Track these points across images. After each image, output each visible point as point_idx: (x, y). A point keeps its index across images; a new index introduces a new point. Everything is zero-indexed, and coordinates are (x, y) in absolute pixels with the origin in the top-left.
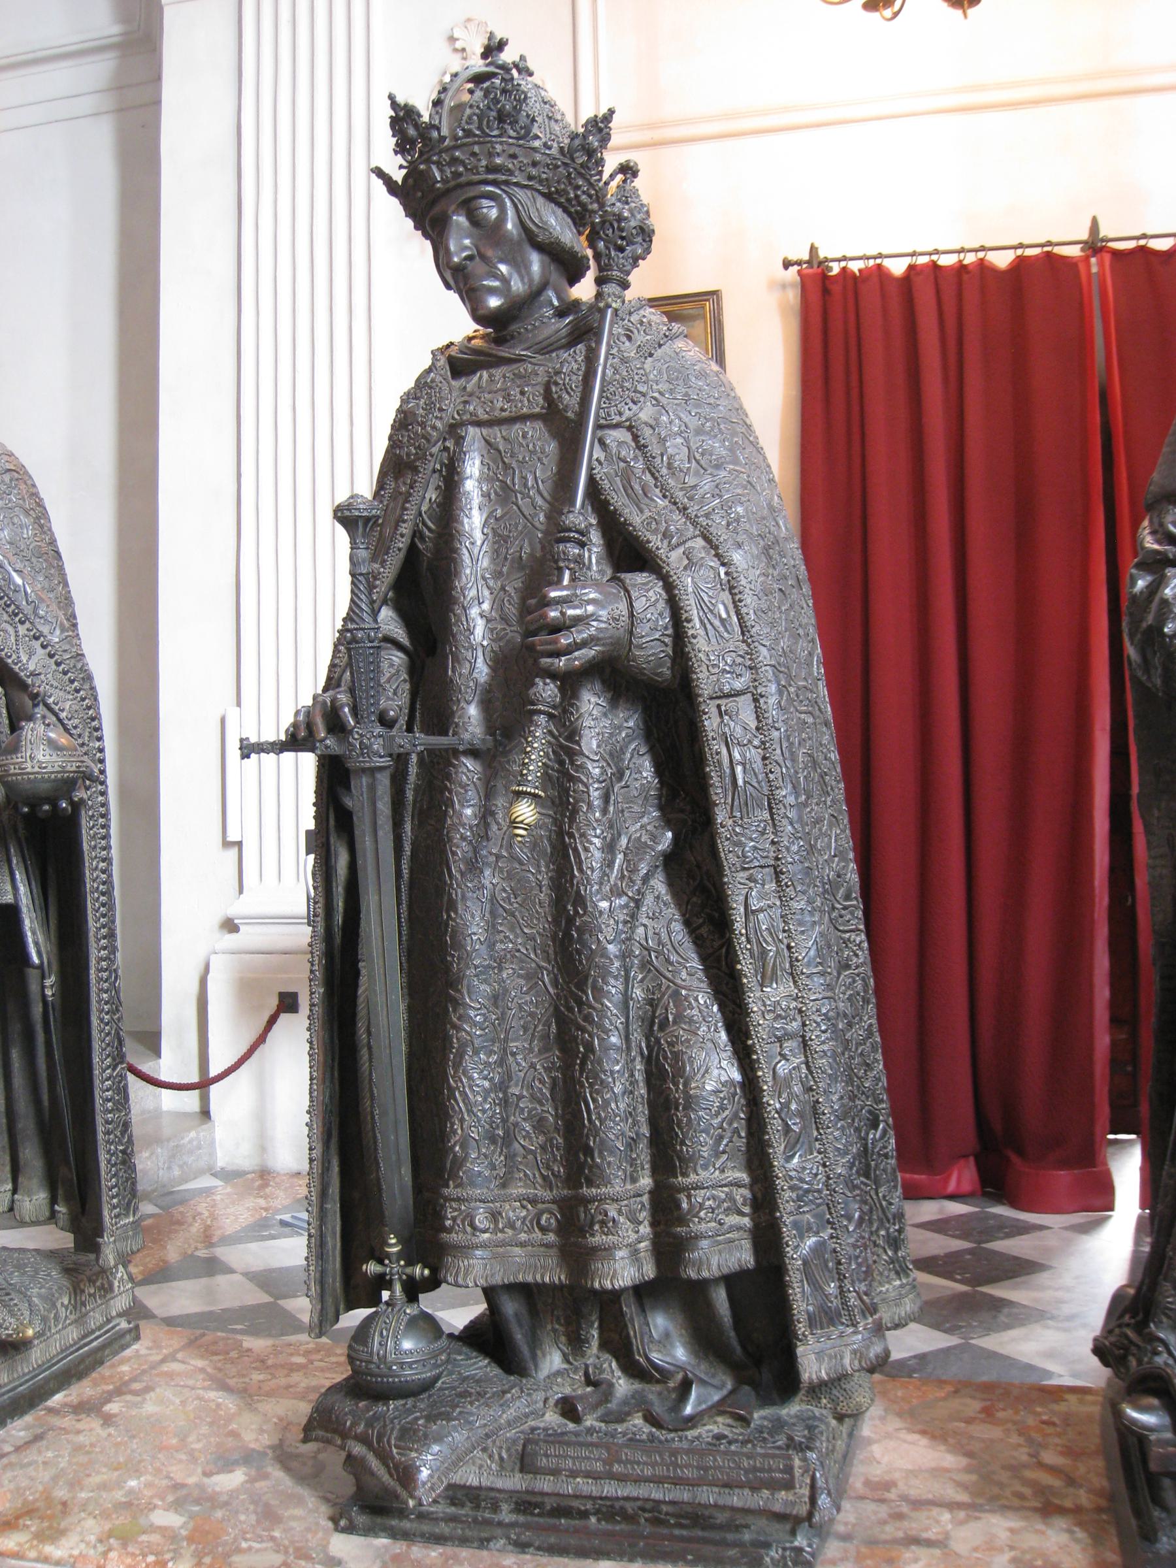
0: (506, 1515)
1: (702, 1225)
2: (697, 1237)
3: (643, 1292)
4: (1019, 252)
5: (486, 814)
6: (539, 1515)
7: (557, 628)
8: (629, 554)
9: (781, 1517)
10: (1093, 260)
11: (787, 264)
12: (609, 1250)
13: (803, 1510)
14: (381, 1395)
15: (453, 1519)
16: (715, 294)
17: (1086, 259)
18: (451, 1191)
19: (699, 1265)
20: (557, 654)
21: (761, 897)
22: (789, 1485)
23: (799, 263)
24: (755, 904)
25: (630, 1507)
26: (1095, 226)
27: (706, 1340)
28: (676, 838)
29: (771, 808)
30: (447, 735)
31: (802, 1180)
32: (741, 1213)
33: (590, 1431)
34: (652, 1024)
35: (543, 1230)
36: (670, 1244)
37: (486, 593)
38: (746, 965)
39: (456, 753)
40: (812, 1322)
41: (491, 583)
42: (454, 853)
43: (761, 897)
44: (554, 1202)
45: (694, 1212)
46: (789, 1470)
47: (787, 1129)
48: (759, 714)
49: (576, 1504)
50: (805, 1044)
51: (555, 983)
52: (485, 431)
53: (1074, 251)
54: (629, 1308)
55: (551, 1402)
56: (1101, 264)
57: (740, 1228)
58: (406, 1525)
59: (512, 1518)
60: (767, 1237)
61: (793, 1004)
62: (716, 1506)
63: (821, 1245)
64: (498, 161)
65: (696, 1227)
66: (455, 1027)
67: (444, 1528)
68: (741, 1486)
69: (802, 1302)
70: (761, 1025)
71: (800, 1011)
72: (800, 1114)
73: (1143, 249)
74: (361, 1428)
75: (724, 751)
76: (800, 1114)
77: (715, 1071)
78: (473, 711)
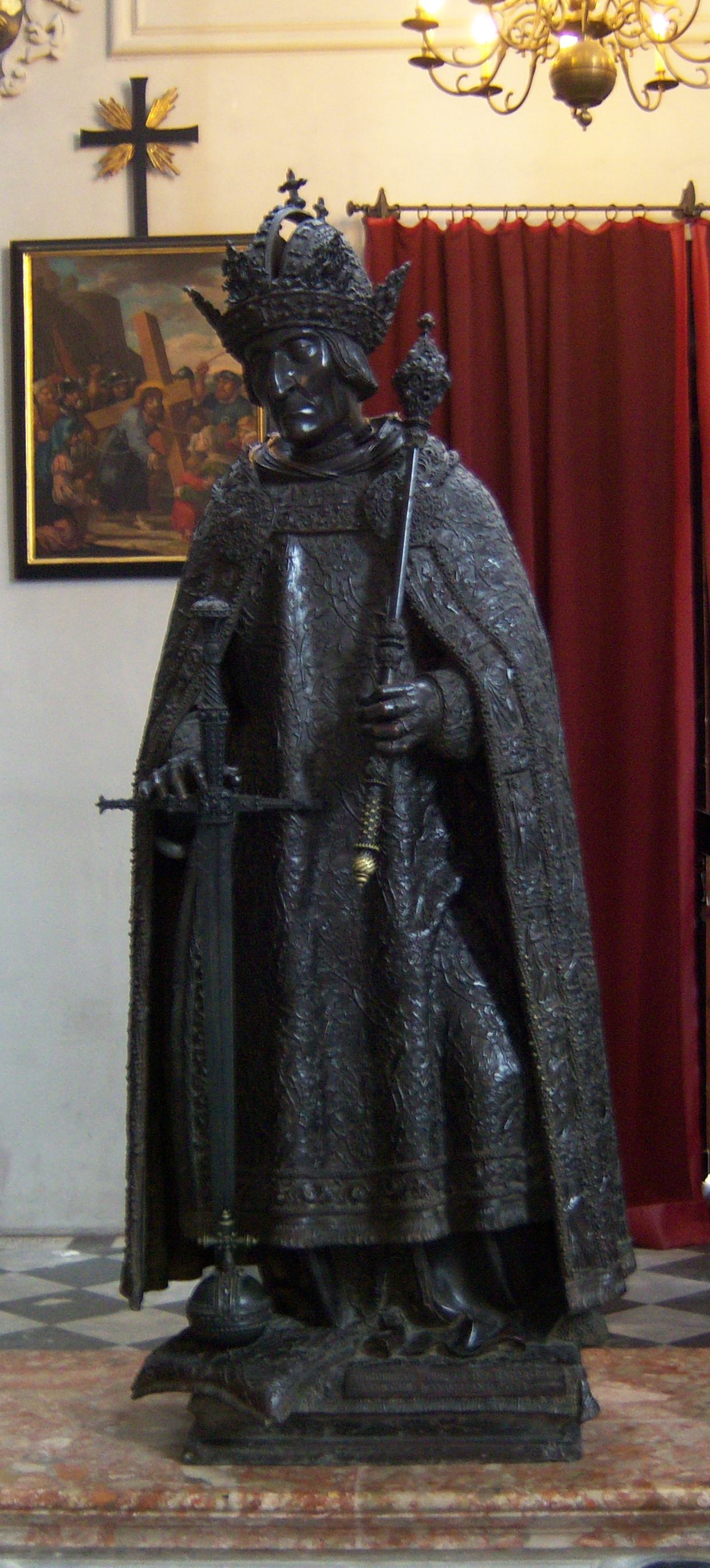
0: (328, 1436)
1: (493, 1188)
2: (491, 1197)
3: (434, 1249)
4: (611, 214)
5: (311, 863)
6: (356, 1435)
7: (391, 718)
8: (432, 653)
9: (553, 1418)
10: (687, 227)
11: (352, 209)
12: (419, 1211)
13: (574, 1410)
14: (221, 1345)
15: (283, 1443)
17: (680, 228)
18: (283, 1170)
19: (491, 1219)
20: (392, 738)
21: (539, 929)
22: (562, 1391)
23: (366, 209)
24: (534, 936)
25: (433, 1421)
26: (690, 192)
27: (480, 1288)
28: (464, 885)
29: (544, 861)
30: (277, 796)
31: (568, 1151)
32: (518, 1179)
33: (398, 1362)
34: (447, 1030)
35: (355, 1201)
36: (465, 1205)
37: (308, 679)
38: (527, 983)
39: (288, 811)
40: (577, 1264)
41: (312, 671)
42: (286, 895)
43: (539, 929)
44: (365, 1176)
45: (487, 1177)
46: (563, 1378)
47: (558, 1111)
48: (537, 787)
49: (389, 1421)
50: (568, 1046)
51: (366, 999)
52: (303, 540)
53: (666, 217)
54: (423, 1264)
55: (361, 1343)
56: (696, 233)
57: (519, 1192)
58: (245, 1451)
59: (333, 1439)
60: (541, 1195)
61: (561, 1014)
62: (505, 1412)
63: (582, 1203)
64: (320, 310)
65: (491, 1189)
66: (284, 1035)
67: (280, 1451)
68: (523, 1394)
69: (569, 1244)
70: (543, 1031)
71: (566, 1019)
72: (565, 1099)
74: (209, 1371)
75: (511, 816)
76: (565, 1099)
77: (502, 1065)
78: (298, 778)
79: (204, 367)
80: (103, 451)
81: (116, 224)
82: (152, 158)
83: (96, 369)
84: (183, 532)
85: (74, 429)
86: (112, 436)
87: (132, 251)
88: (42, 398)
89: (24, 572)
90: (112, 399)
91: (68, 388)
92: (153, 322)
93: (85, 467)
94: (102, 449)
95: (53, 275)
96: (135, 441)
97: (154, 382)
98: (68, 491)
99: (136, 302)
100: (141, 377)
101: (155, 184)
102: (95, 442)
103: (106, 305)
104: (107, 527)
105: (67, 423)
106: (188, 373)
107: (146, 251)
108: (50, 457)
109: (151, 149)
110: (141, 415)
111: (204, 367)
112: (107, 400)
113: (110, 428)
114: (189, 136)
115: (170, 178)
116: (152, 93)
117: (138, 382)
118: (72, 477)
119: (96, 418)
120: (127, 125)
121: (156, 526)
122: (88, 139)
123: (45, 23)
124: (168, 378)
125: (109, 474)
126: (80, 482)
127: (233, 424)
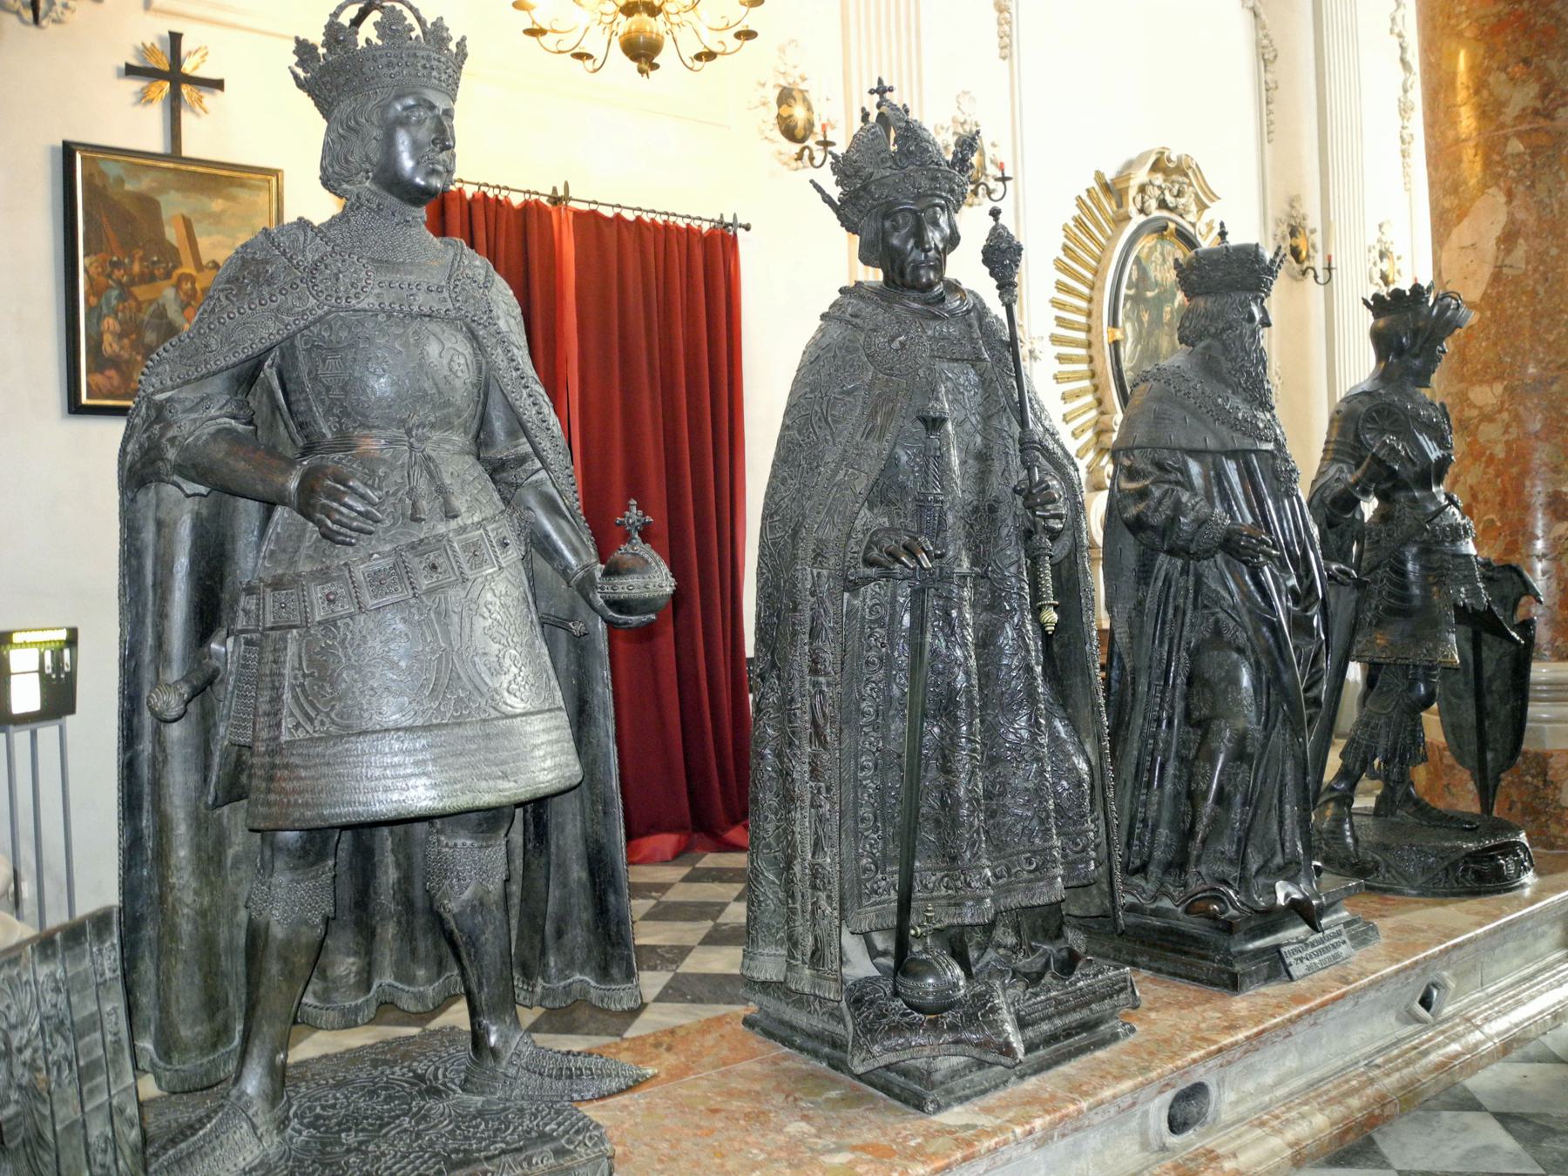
16: (275, 173)
73: (594, 212)
80: (146, 318)
81: (152, 139)
83: (141, 253)
85: (122, 298)
87: (171, 165)
89: (75, 407)
91: (115, 265)
92: (188, 224)
93: (130, 329)
94: (145, 316)
95: (103, 175)
96: (173, 312)
97: (188, 268)
98: (116, 347)
99: (173, 206)
100: (178, 263)
101: (186, 118)
102: (139, 309)
103: (148, 205)
105: (115, 293)
107: (183, 167)
108: (100, 318)
109: (185, 90)
112: (148, 278)
113: (151, 302)
114: (218, 85)
115: (198, 115)
116: (186, 46)
117: (175, 267)
118: (120, 336)
119: (141, 292)
120: (164, 65)
122: (130, 71)
126: (126, 341)
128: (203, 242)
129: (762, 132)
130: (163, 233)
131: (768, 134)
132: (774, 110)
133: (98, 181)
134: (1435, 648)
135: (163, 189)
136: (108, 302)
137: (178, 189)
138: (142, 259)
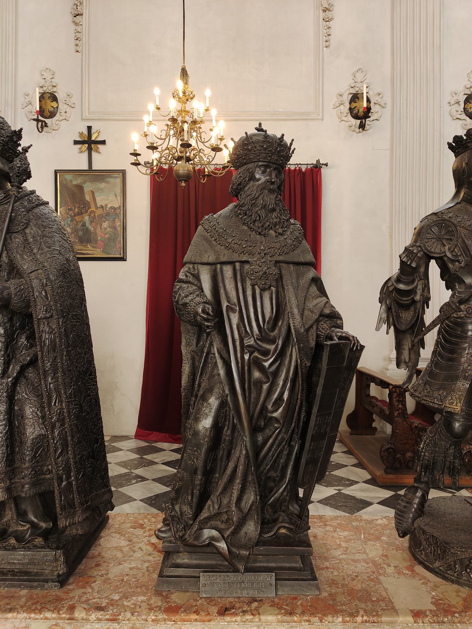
79: (106, 205)
82: (93, 148)
84: (100, 249)
86: (82, 222)
88: (62, 212)
90: (82, 213)
91: (70, 210)
96: (88, 225)
99: (88, 187)
103: (80, 188)
104: (80, 247)
106: (102, 206)
109: (93, 146)
110: (89, 217)
111: (106, 205)
112: (80, 213)
114: (103, 142)
116: (93, 131)
119: (78, 218)
121: (93, 247)
122: (76, 142)
123: (64, 110)
124: (97, 208)
125: (81, 233)
127: (114, 220)
128: (98, 199)
129: (340, 118)
130: (85, 198)
131: (345, 119)
132: (348, 106)
133: (64, 182)
134: (446, 397)
135: (84, 182)
136: (67, 223)
137: (91, 181)
138: (79, 207)
